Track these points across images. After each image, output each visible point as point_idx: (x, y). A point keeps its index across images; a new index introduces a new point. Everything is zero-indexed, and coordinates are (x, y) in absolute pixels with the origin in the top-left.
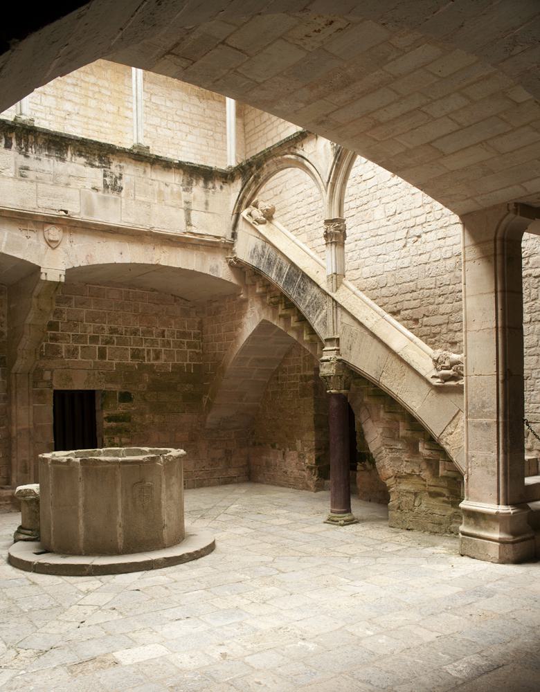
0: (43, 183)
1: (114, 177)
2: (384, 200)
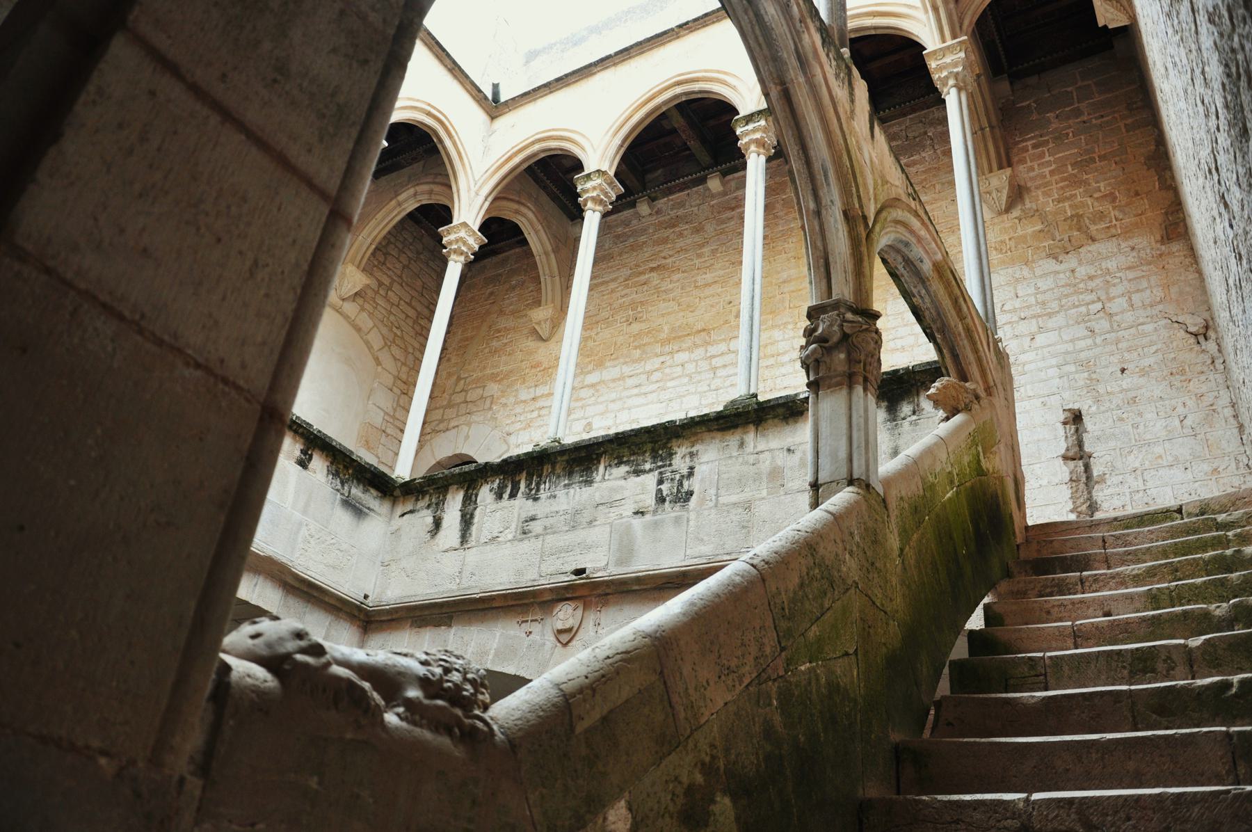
0: (554, 533)
1: (678, 477)
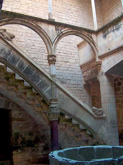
2: (29, 51)
